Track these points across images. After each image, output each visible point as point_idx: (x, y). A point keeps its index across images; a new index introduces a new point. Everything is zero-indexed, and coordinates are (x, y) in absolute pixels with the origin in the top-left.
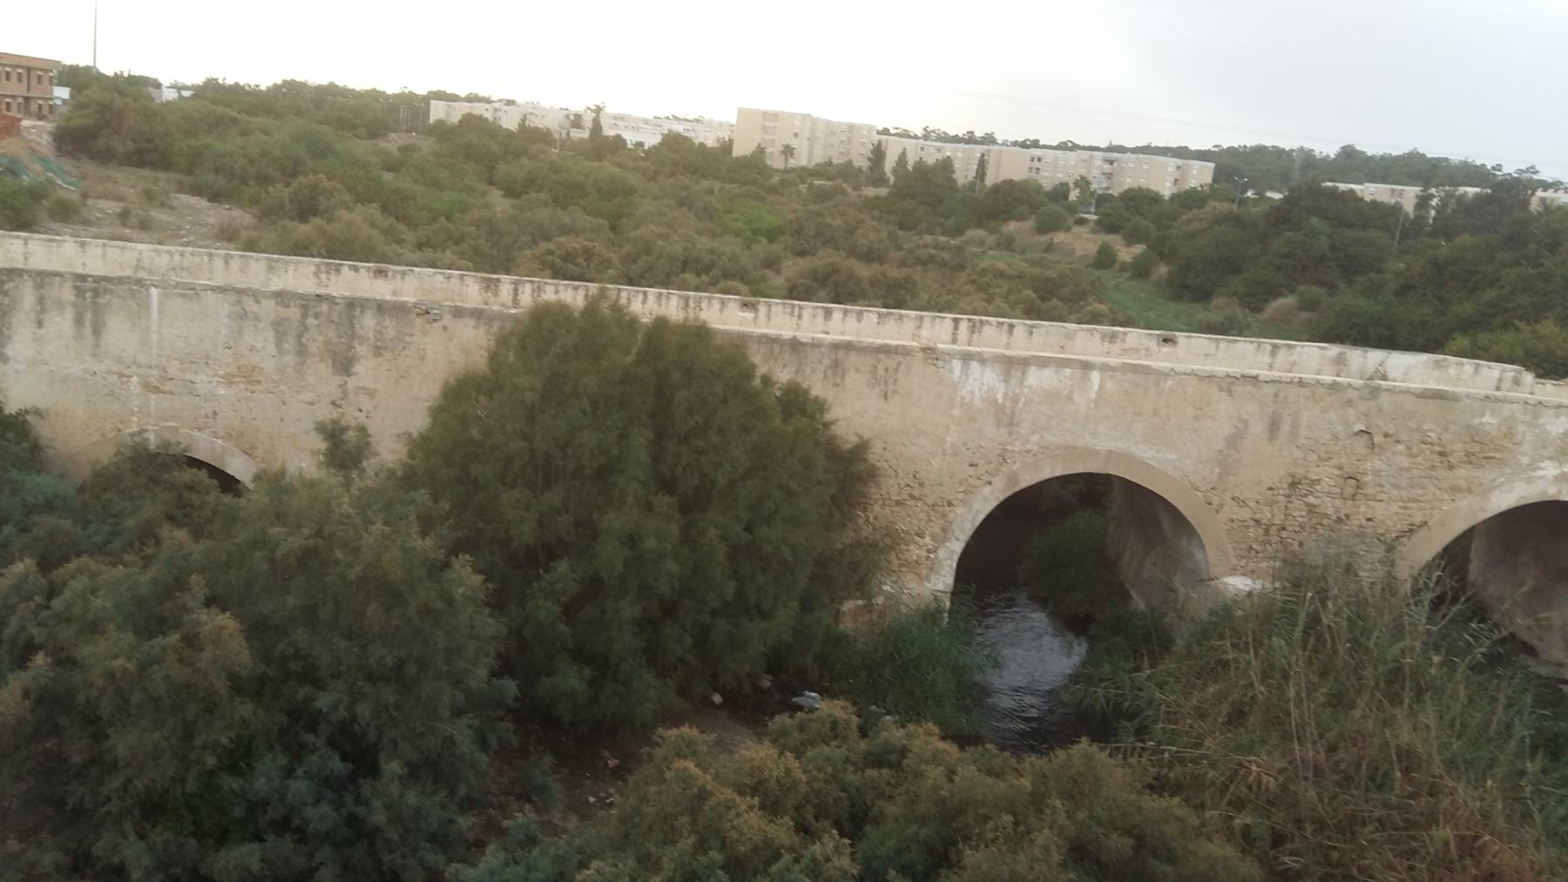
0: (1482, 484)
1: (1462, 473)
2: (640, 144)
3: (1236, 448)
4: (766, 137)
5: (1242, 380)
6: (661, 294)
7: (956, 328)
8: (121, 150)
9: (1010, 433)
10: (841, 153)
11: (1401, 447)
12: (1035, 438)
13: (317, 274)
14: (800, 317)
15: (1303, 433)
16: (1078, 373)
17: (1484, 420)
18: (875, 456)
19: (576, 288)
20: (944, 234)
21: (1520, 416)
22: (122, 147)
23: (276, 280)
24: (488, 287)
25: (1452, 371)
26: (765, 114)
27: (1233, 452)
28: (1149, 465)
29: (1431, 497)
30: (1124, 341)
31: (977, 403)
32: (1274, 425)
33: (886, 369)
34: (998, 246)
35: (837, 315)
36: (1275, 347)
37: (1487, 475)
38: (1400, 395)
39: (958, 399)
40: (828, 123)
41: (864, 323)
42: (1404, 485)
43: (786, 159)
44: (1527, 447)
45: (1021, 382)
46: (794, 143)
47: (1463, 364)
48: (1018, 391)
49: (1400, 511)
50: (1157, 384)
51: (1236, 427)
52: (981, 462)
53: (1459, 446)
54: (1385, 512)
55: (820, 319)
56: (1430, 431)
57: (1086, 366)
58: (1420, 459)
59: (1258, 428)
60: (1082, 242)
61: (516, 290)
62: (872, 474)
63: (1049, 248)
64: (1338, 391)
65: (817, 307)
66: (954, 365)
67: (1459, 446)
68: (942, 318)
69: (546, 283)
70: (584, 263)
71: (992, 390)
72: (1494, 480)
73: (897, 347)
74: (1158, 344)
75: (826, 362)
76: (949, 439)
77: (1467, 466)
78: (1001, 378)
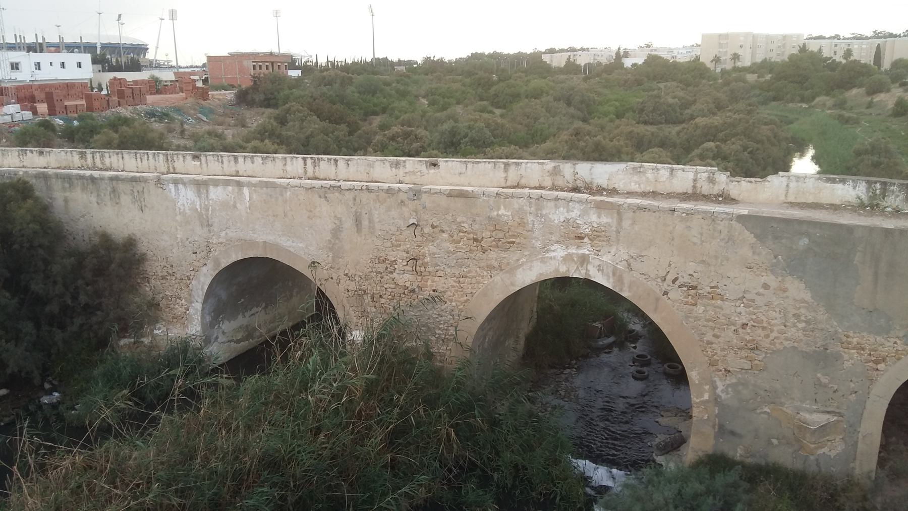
0: (508, 264)
1: (493, 255)
2: (634, 65)
3: (338, 238)
4: (721, 50)
5: (332, 189)
6: (154, 154)
7: (305, 164)
8: (257, 99)
9: (210, 231)
10: (778, 55)
11: (445, 235)
12: (223, 234)
13: (19, 155)
14: (222, 162)
15: (378, 226)
16: (236, 189)
17: (500, 213)
18: (143, 248)
19: (117, 154)
20: (803, 100)
21: (527, 208)
22: (259, 97)
23: (5, 160)
24: (82, 157)
25: (650, 175)
26: (720, 35)
27: (337, 242)
28: (290, 251)
29: (474, 274)
30: (404, 166)
31: (187, 211)
32: (358, 221)
33: (138, 191)
34: (834, 106)
35: (241, 160)
36: (507, 165)
37: (512, 256)
38: (436, 195)
39: (178, 210)
40: (768, 37)
41: (255, 164)
42: (453, 265)
43: (735, 63)
44: (537, 233)
45: (207, 197)
46: (740, 52)
47: (658, 169)
48: (206, 203)
49: (455, 284)
50: (282, 195)
51: (335, 223)
52: (198, 251)
53: (487, 234)
54: (444, 285)
55: (233, 162)
56: (464, 222)
57: (239, 184)
58: (462, 243)
59: (349, 224)
60: (888, 99)
61: (93, 157)
62: (142, 259)
63: (870, 105)
64: (393, 195)
65: (230, 156)
66: (170, 187)
67: (487, 234)
68: (297, 158)
69: (105, 152)
70: (402, 141)
71: (193, 203)
72: (518, 260)
73: (139, 177)
74: (427, 167)
75: (109, 189)
76: (178, 236)
77: (496, 250)
78: (196, 194)
